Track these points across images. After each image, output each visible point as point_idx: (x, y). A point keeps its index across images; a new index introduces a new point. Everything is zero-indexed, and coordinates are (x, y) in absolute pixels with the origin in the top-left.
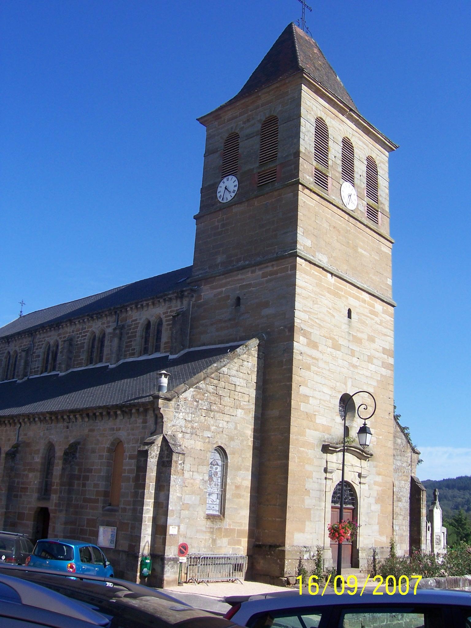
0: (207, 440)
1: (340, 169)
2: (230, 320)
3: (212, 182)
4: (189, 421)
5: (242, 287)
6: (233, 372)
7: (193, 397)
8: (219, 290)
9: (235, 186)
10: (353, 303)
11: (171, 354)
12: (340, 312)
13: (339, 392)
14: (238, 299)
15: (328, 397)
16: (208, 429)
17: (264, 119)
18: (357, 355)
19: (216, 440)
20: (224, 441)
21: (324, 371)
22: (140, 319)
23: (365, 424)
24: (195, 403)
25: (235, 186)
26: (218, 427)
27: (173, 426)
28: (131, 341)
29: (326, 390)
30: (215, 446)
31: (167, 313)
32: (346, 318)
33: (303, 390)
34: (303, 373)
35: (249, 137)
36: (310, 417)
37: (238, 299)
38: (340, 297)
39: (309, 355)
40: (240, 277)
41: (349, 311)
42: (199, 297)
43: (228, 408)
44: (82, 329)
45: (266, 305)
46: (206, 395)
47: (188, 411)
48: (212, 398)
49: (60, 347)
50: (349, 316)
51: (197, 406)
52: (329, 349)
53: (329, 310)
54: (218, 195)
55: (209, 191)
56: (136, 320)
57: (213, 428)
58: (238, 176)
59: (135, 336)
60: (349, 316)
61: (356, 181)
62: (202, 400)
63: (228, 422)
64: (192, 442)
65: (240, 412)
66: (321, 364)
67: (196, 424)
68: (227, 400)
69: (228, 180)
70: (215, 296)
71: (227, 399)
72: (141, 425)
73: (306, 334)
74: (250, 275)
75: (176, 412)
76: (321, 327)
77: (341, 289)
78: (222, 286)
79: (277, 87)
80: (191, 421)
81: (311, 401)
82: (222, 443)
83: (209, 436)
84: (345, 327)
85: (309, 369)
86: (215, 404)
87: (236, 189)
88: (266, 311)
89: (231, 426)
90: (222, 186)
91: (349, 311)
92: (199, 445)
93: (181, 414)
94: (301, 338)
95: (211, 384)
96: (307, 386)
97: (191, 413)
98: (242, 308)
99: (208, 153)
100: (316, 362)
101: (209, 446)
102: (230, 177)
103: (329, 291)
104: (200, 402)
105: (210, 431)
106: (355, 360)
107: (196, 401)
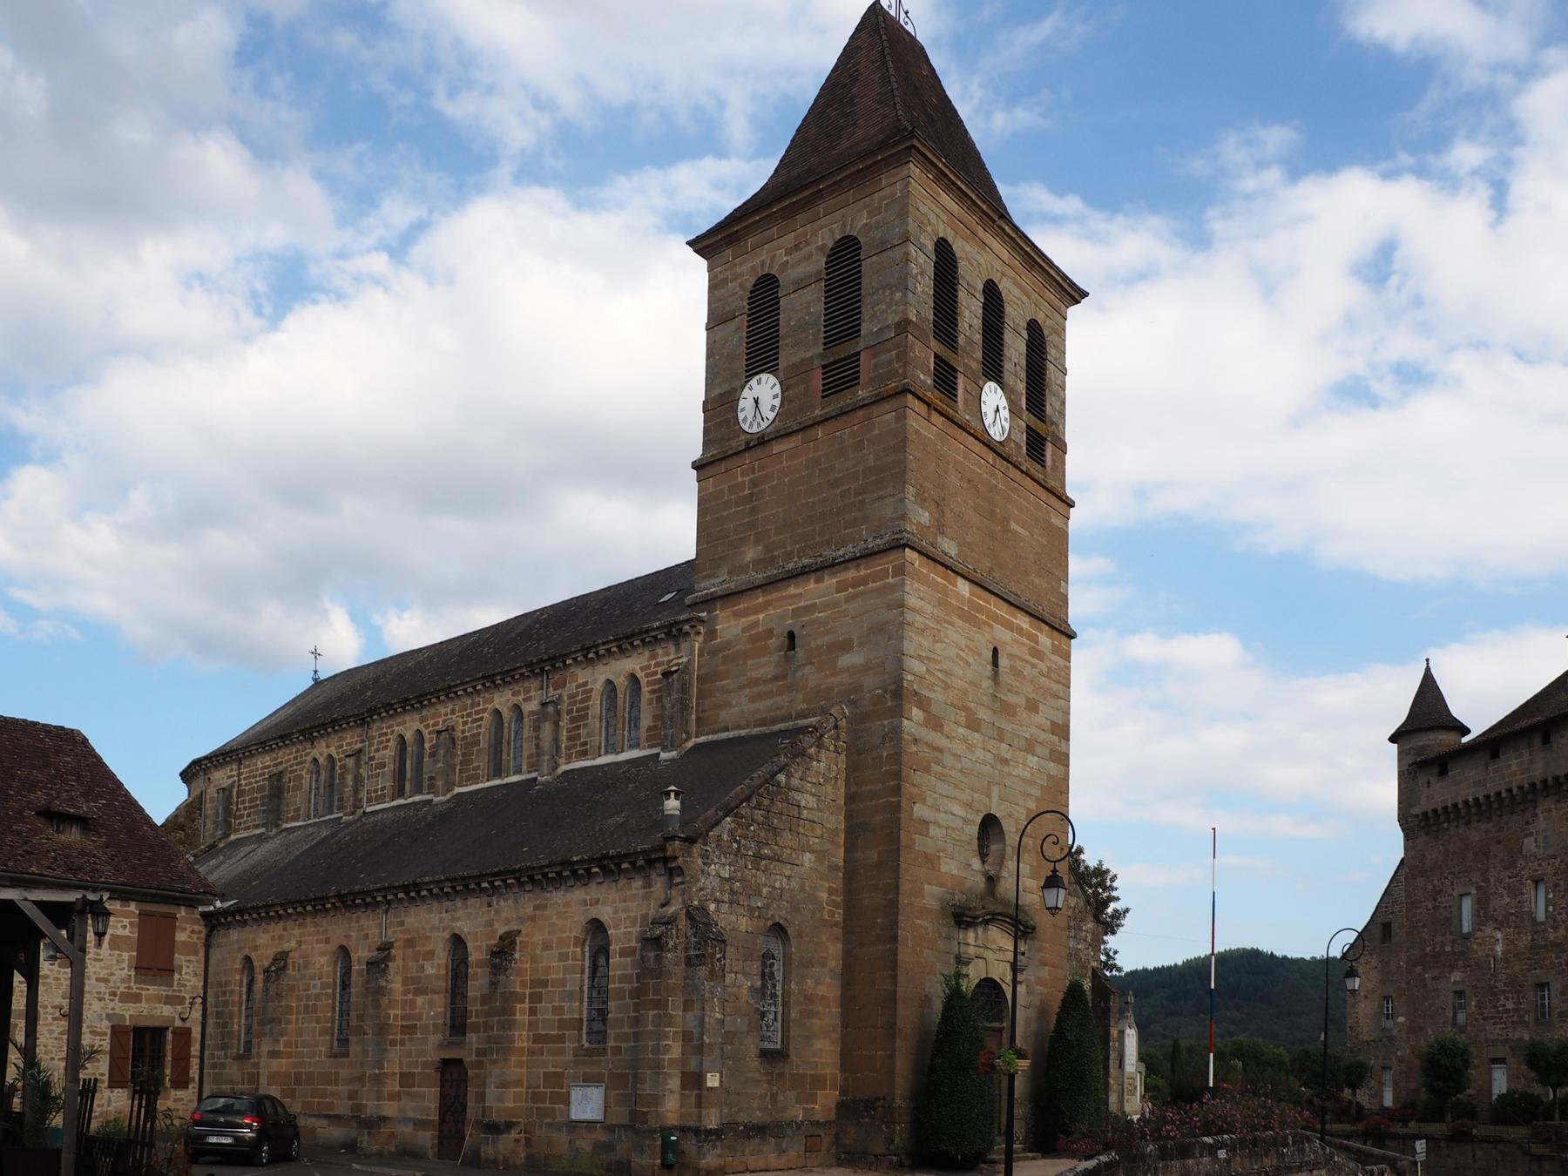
1: (979, 355)
2: (776, 679)
3: (726, 388)
5: (797, 613)
6: (795, 782)
7: (731, 833)
8: (752, 618)
9: (775, 397)
10: (1002, 635)
11: (664, 750)
12: (980, 655)
13: (978, 811)
14: (791, 635)
15: (960, 822)
17: (831, 245)
18: (1007, 736)
21: (953, 773)
22: (595, 681)
23: (1054, 871)
25: (775, 397)
26: (773, 887)
28: (578, 727)
29: (957, 809)
30: (770, 923)
31: (648, 667)
32: (989, 667)
33: (919, 811)
34: (919, 778)
35: (800, 285)
36: (931, 861)
37: (791, 635)
38: (977, 624)
40: (792, 590)
41: (995, 651)
42: (712, 634)
44: (473, 706)
45: (846, 646)
49: (427, 746)
50: (995, 663)
52: (961, 730)
54: (741, 416)
55: (720, 407)
56: (586, 684)
57: (765, 890)
58: (781, 374)
59: (586, 716)
60: (995, 663)
61: (1008, 378)
62: (746, 838)
63: (789, 878)
64: (734, 918)
65: (808, 858)
66: (948, 760)
68: (787, 839)
69: (759, 382)
70: (744, 630)
71: (787, 835)
72: (641, 892)
73: (923, 703)
74: (812, 585)
76: (947, 687)
77: (980, 609)
78: (758, 610)
79: (859, 171)
81: (933, 831)
85: (927, 770)
87: (777, 402)
88: (846, 660)
89: (793, 883)
90: (747, 395)
91: (995, 651)
92: (744, 923)
94: (915, 711)
95: (759, 806)
96: (924, 802)
98: (800, 653)
99: (716, 321)
101: (761, 924)
102: (764, 376)
103: (963, 615)
106: (1004, 747)
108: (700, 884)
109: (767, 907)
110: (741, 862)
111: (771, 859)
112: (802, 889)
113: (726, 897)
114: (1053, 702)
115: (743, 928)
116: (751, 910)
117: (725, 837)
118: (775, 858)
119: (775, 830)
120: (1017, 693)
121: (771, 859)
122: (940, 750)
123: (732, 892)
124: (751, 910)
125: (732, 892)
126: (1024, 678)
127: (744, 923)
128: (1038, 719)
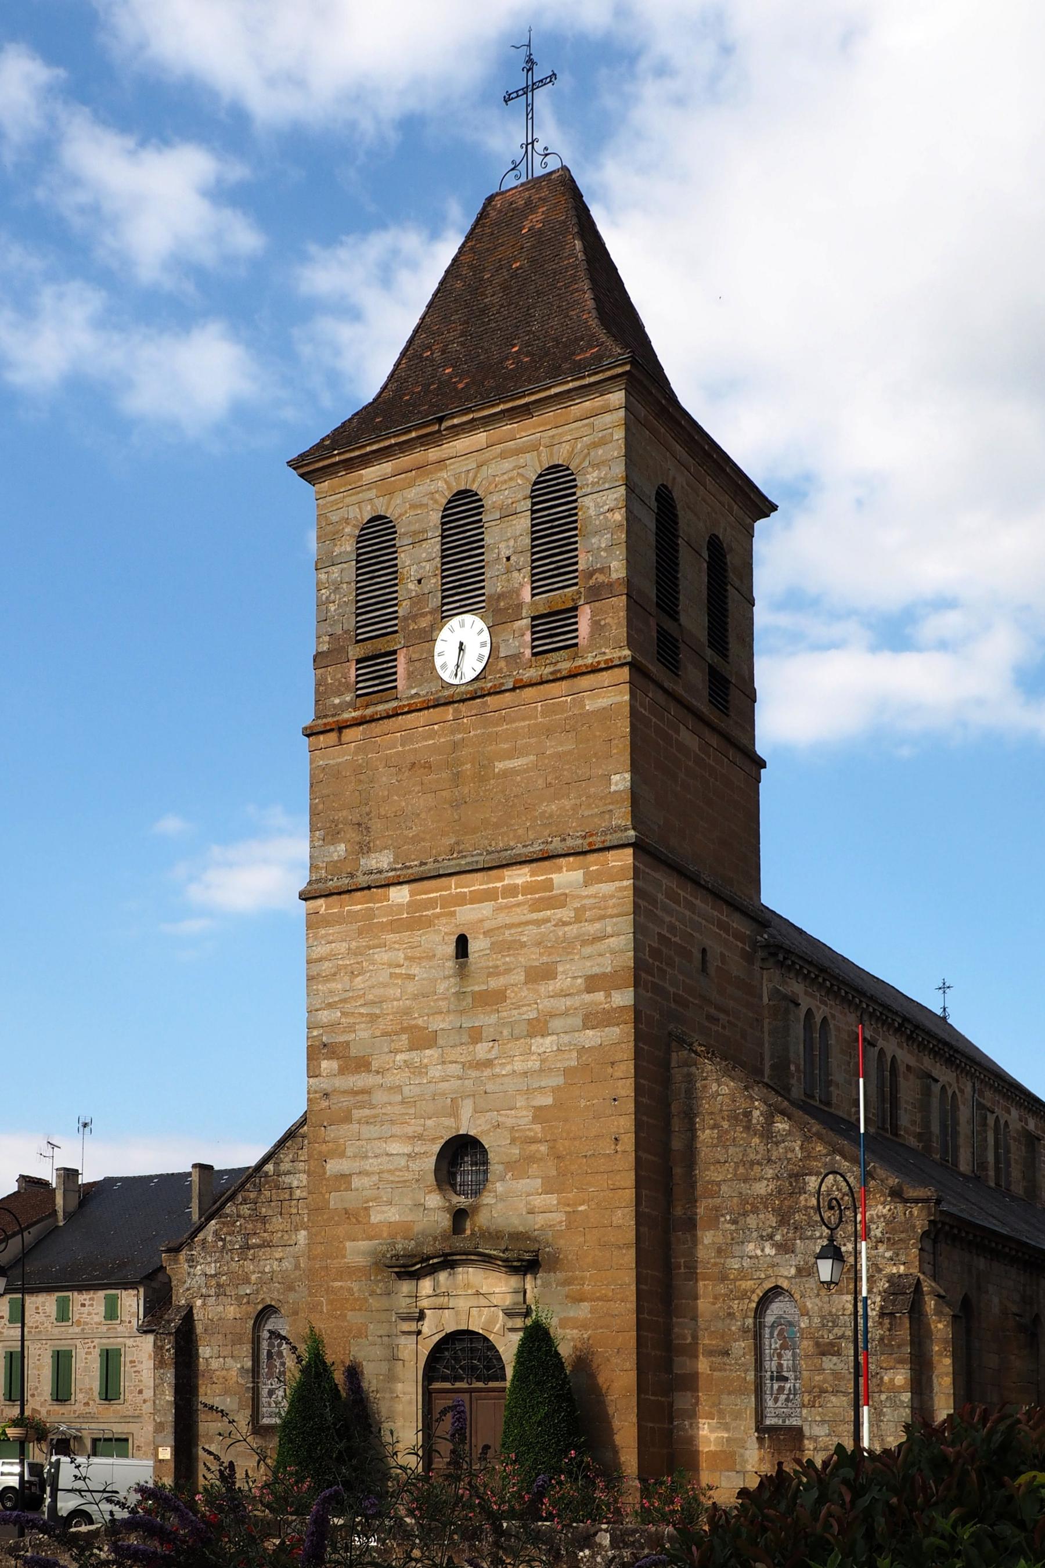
0: (245, 1300)
4: (211, 1276)
7: (216, 1233)
16: (247, 1281)
19: (260, 1297)
20: (275, 1295)
24: (220, 1243)
26: (263, 1272)
27: (188, 1289)
39: (344, 1092)
41: (462, 944)
43: (280, 1234)
46: (238, 1223)
47: (209, 1259)
48: (250, 1226)
51: (224, 1246)
53: (397, 971)
57: (253, 1277)
63: (280, 1260)
64: (221, 1308)
67: (224, 1278)
75: (190, 1267)
80: (215, 1275)
82: (272, 1299)
83: (248, 1292)
84: (446, 986)
85: (347, 1119)
86: (255, 1234)
89: (286, 1264)
91: (462, 944)
93: (199, 1267)
97: (215, 1262)
100: (366, 1097)
101: (250, 1309)
104: (228, 1238)
105: (250, 1283)
107: (221, 1240)
108: (187, 1285)
109: (257, 1292)
110: (227, 1257)
111: (259, 1246)
112: (297, 1267)
113: (212, 1292)
114: (588, 950)
115: (231, 1316)
116: (239, 1298)
117: (210, 1239)
118: (266, 1245)
119: (264, 1220)
120: (508, 971)
121: (259, 1246)
122: (363, 1092)
123: (219, 1285)
124: (239, 1298)
125: (219, 1285)
126: (523, 945)
127: (232, 1311)
128: (560, 983)
